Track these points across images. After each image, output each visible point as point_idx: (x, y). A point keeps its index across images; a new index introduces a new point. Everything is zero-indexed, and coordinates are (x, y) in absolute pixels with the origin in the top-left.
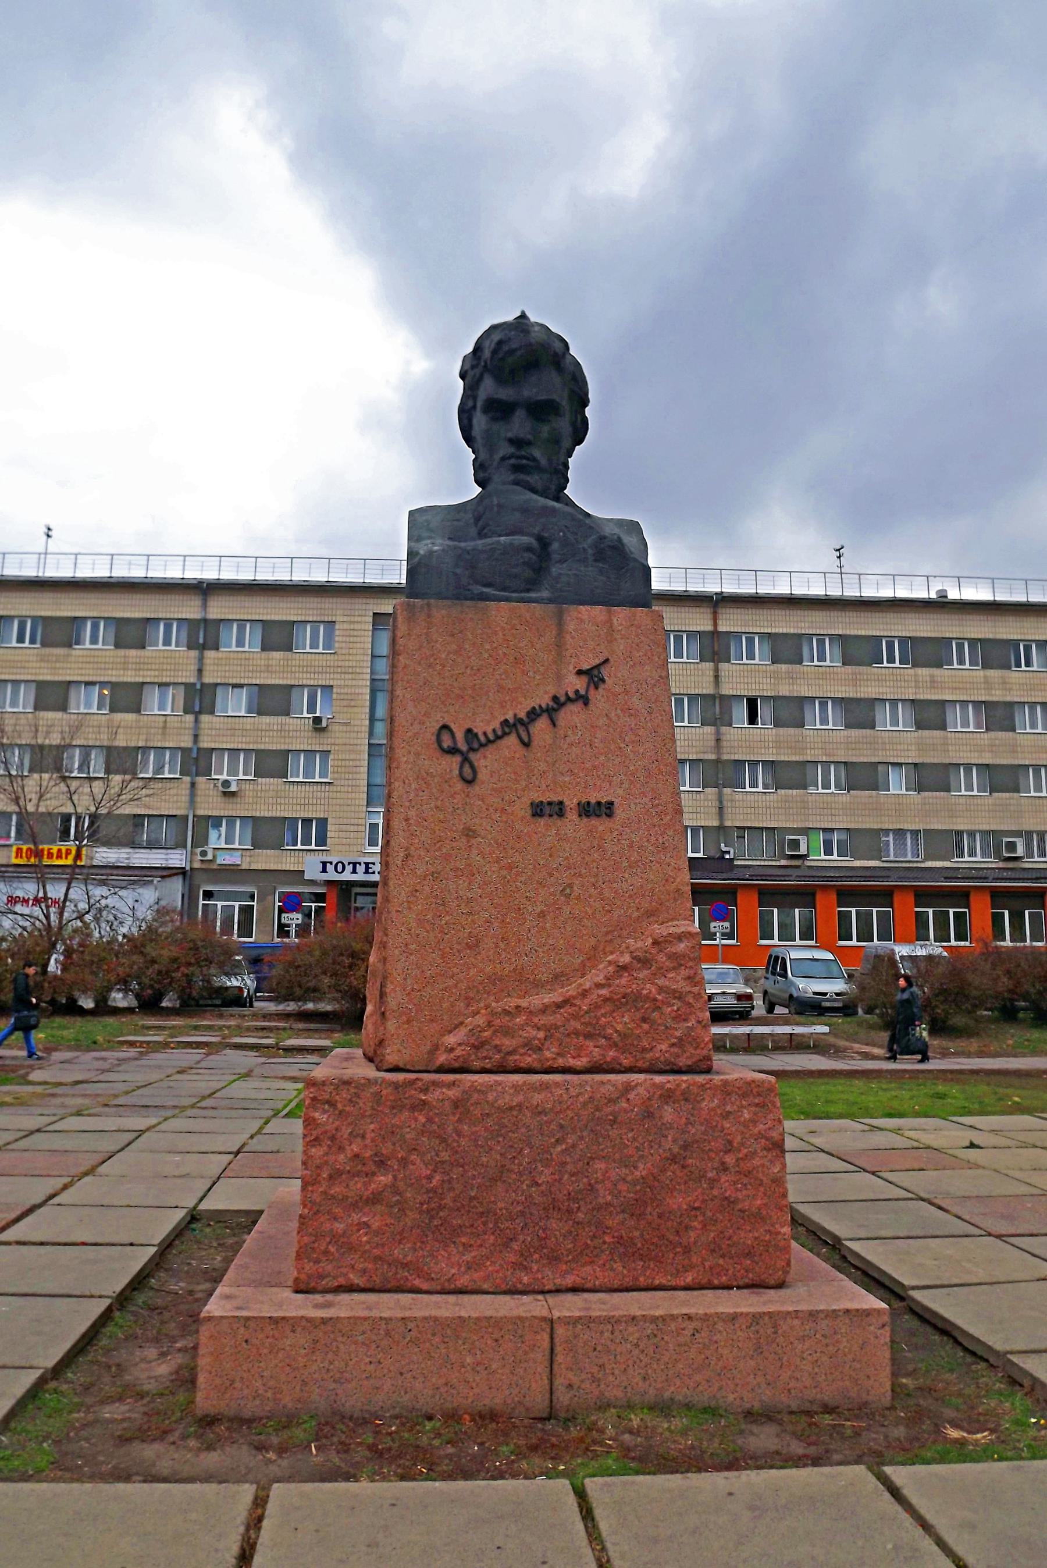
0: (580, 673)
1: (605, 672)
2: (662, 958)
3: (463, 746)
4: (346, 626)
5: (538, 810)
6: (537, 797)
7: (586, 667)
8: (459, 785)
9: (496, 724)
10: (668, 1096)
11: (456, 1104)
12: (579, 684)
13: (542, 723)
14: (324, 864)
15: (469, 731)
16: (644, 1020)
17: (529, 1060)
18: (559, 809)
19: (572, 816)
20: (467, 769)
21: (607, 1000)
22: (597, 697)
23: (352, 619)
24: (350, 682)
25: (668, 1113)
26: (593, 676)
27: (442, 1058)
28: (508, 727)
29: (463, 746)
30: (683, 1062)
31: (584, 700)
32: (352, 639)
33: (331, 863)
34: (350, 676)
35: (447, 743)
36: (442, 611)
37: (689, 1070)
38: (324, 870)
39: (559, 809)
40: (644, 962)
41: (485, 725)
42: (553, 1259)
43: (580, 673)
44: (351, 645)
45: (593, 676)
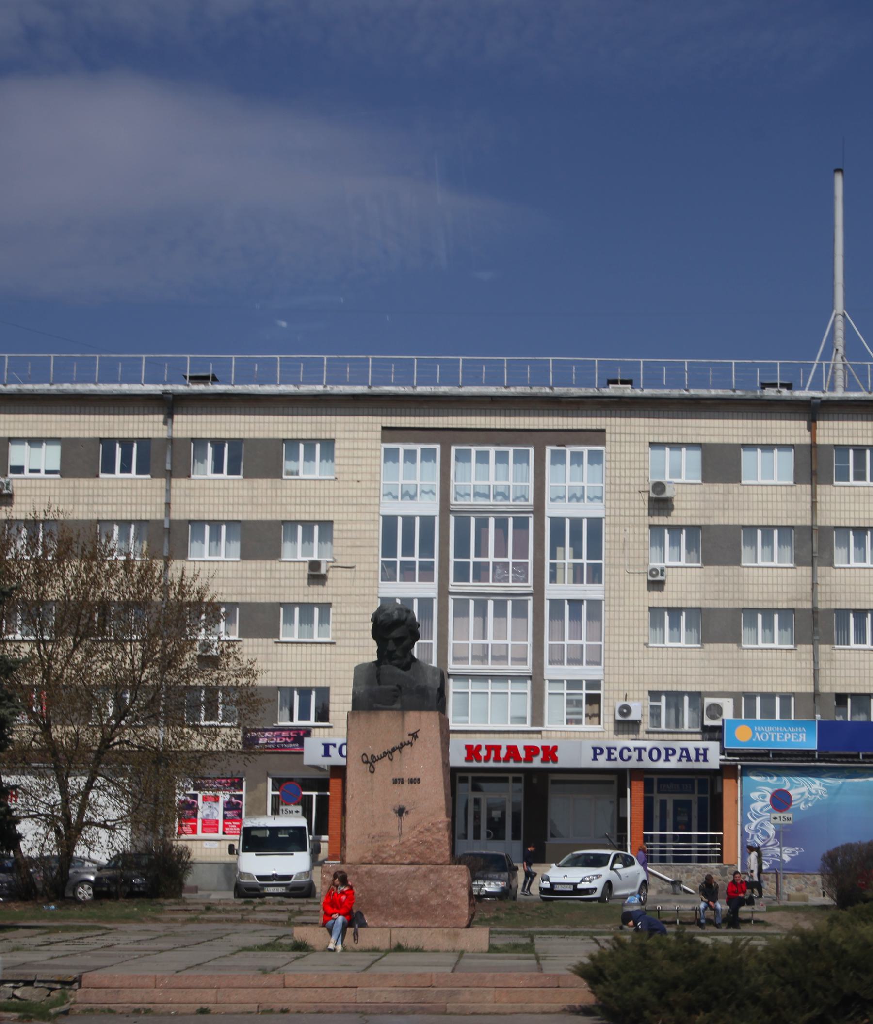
0: (409, 735)
1: (418, 734)
2: (434, 829)
3: (370, 760)
4: (347, 445)
5: (395, 781)
6: (395, 777)
7: (412, 732)
8: (369, 774)
9: (382, 753)
10: (431, 871)
11: (366, 873)
12: (410, 738)
13: (397, 752)
14: (327, 746)
15: (372, 756)
16: (428, 848)
17: (391, 861)
18: (402, 781)
19: (406, 783)
20: (372, 769)
21: (415, 842)
22: (416, 743)
23: (356, 435)
24: (354, 517)
25: (432, 876)
26: (414, 735)
27: (364, 860)
28: (385, 754)
29: (370, 760)
30: (439, 861)
31: (410, 743)
32: (355, 461)
33: (334, 745)
34: (354, 509)
35: (365, 759)
36: (363, 715)
37: (441, 864)
38: (327, 754)
39: (402, 781)
40: (428, 830)
41: (377, 754)
42: (395, 918)
43: (409, 735)
44: (355, 469)
45: (414, 735)
